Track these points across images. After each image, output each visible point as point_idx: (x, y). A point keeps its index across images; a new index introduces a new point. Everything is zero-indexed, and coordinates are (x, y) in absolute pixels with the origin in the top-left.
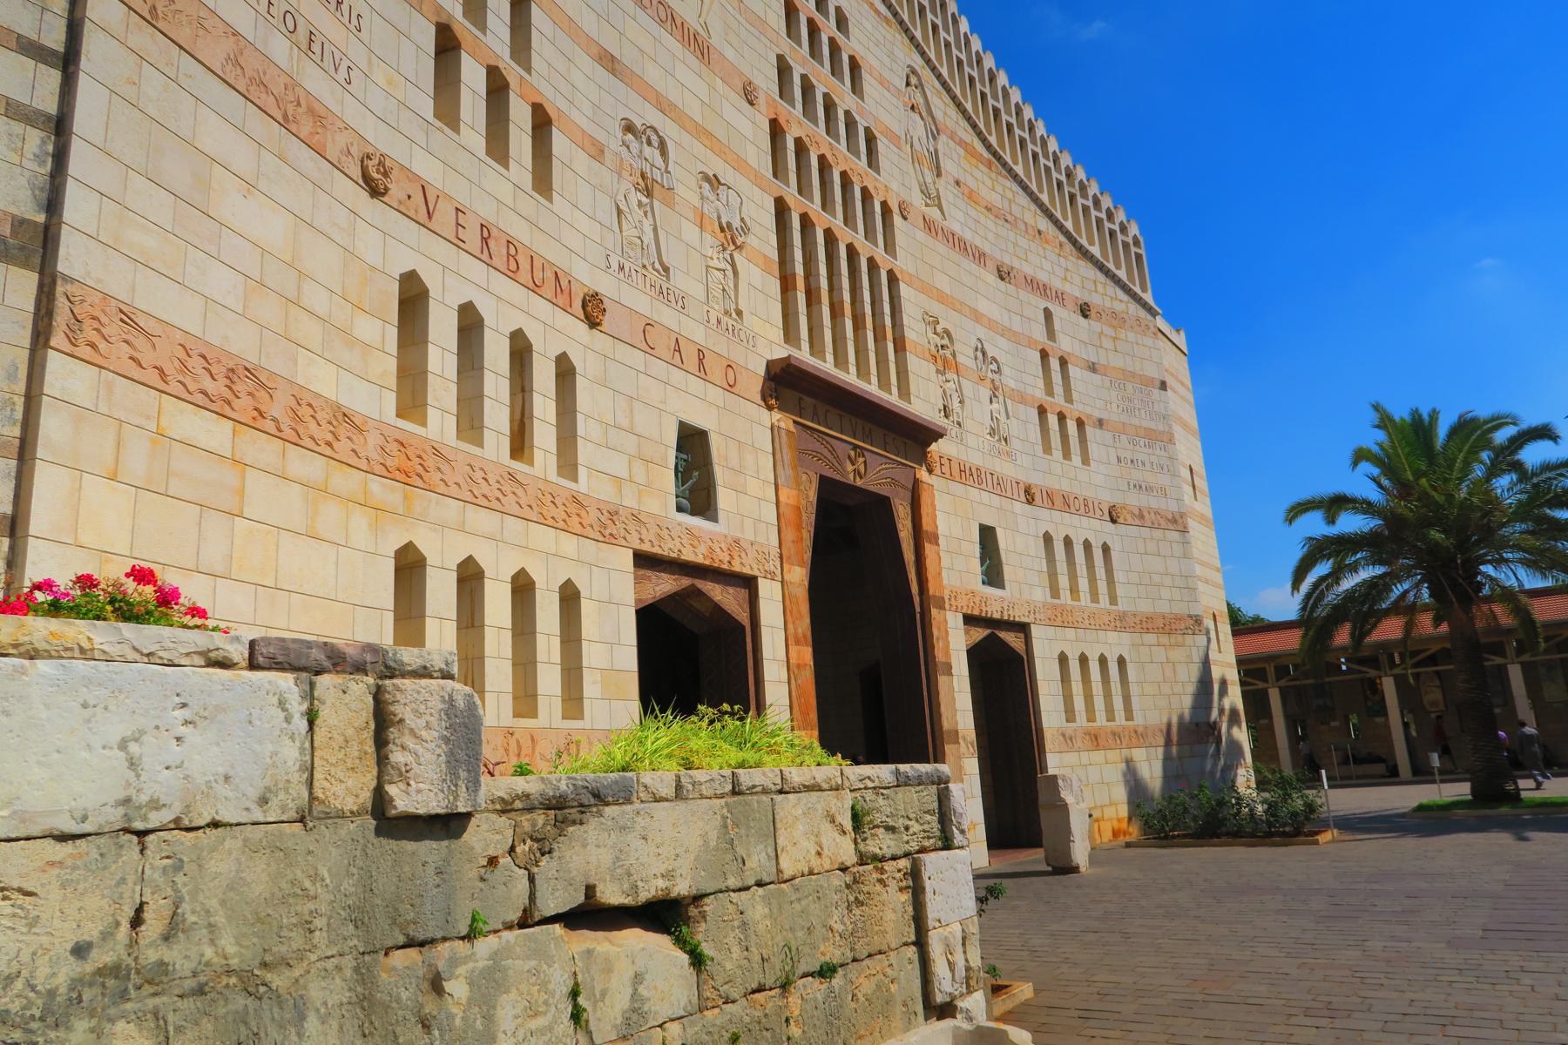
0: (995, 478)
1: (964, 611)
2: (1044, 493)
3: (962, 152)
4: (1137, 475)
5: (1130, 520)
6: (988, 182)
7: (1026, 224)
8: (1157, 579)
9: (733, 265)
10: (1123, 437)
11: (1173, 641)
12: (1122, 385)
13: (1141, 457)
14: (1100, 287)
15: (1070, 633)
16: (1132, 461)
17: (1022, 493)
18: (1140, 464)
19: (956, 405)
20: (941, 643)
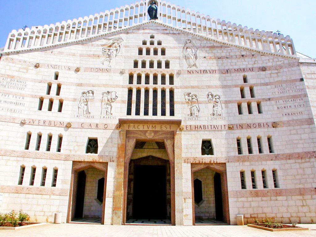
0: (212, 127)
1: (192, 162)
2: (238, 126)
3: (208, 49)
4: (286, 111)
5: (282, 125)
6: (221, 51)
7: (236, 56)
8: (295, 142)
9: (110, 105)
10: (281, 101)
11: (303, 161)
12: (281, 86)
13: (289, 105)
14: (271, 61)
15: (247, 163)
16: (285, 107)
17: (227, 128)
18: (289, 107)
19: (196, 112)
20: (178, 171)
